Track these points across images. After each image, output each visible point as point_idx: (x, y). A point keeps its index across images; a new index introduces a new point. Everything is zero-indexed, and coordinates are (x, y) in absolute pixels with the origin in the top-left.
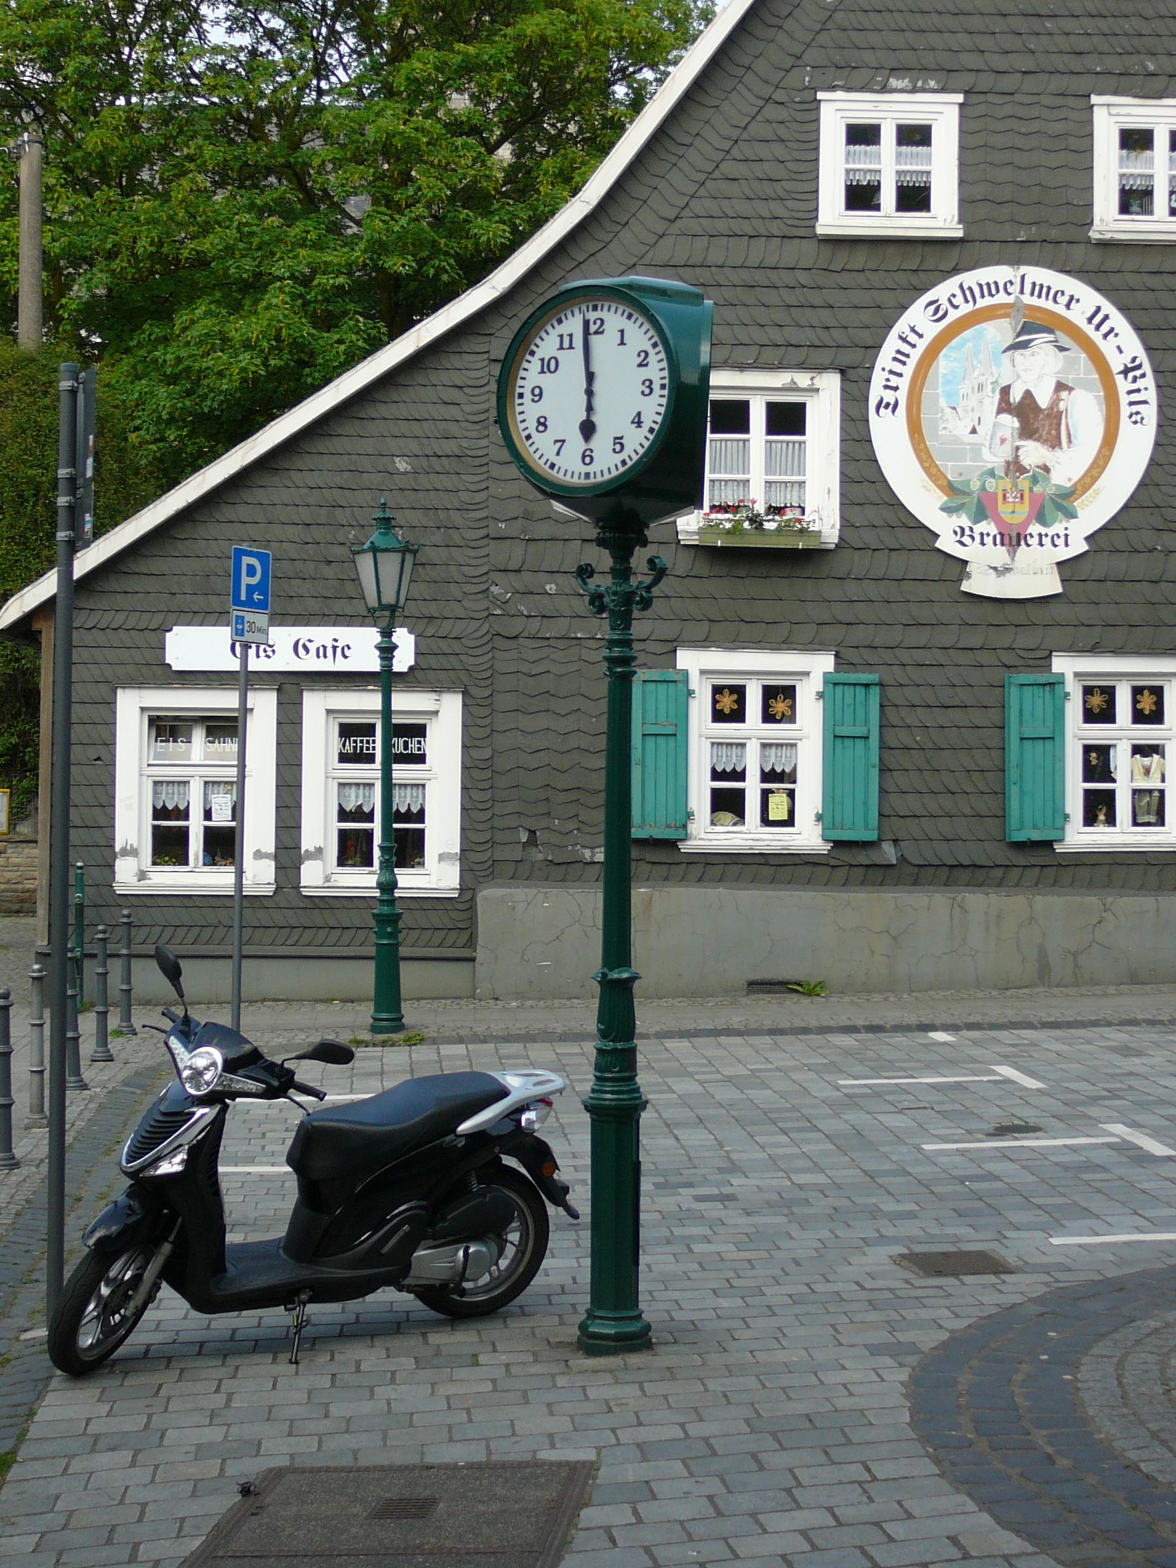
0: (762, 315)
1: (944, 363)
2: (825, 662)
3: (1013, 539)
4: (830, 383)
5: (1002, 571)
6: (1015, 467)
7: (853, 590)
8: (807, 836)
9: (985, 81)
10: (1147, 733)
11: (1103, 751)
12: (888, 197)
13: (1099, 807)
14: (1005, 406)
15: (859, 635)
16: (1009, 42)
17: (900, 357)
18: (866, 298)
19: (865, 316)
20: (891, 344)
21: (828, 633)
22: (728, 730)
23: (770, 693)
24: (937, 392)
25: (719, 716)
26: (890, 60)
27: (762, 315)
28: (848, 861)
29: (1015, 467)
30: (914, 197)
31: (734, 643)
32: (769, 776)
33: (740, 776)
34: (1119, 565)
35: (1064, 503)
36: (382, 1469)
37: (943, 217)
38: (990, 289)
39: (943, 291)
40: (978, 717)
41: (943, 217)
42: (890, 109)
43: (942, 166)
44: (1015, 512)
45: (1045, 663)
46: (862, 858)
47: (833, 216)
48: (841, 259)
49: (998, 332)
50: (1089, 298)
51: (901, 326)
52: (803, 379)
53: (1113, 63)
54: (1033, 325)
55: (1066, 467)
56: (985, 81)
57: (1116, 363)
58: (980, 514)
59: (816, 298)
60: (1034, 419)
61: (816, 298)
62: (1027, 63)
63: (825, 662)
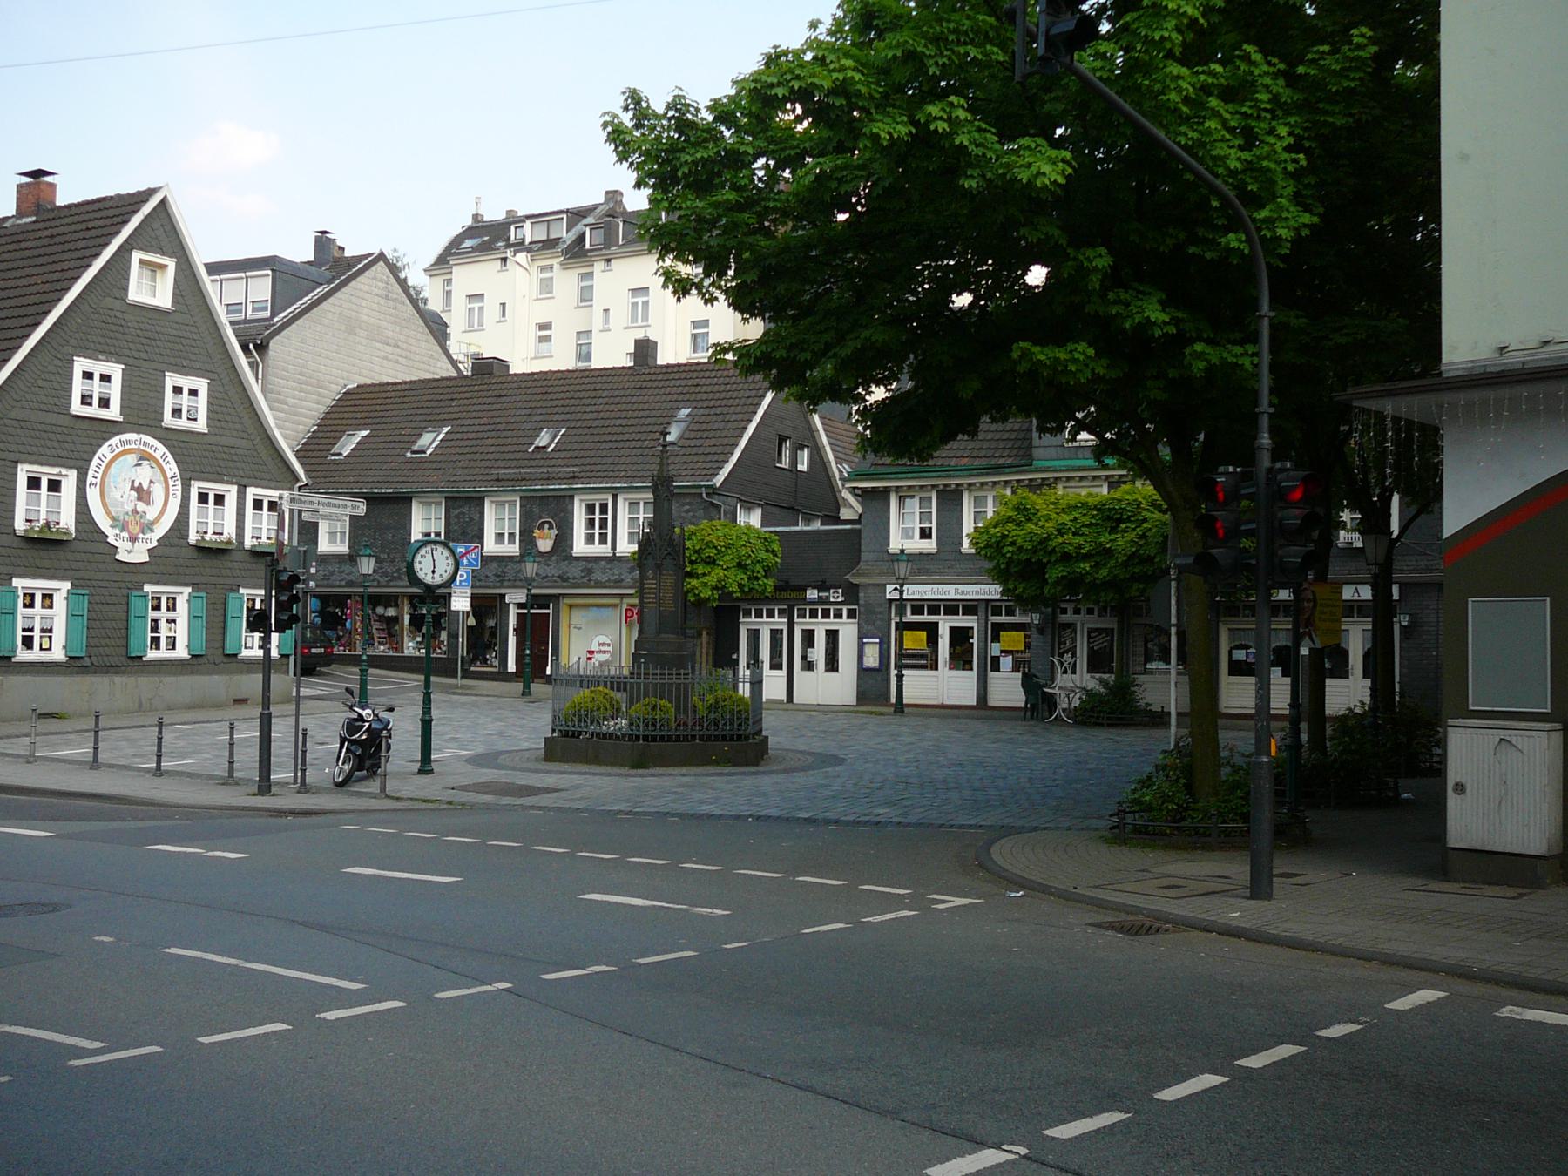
0: (49, 444)
1: (113, 469)
2: (67, 585)
3: (133, 540)
4: (73, 473)
5: (129, 552)
6: (135, 512)
7: (78, 556)
8: (58, 654)
9: (131, 361)
10: (171, 615)
11: (155, 621)
12: (96, 401)
13: (156, 642)
14: (133, 488)
15: (78, 574)
16: (140, 347)
17: (99, 466)
18: (86, 441)
19: (87, 448)
20: (95, 460)
21: (69, 573)
22: (29, 611)
23: (44, 596)
24: (110, 481)
25: (25, 606)
26: (100, 347)
27: (49, 444)
28: (74, 665)
29: (135, 512)
30: (104, 403)
31: (34, 576)
32: (43, 631)
33: (32, 630)
34: (167, 551)
35: (149, 527)
36: (221, 808)
37: (114, 412)
38: (130, 442)
39: (114, 441)
40: (119, 608)
41: (114, 412)
42: (98, 367)
43: (115, 391)
44: (135, 529)
45: (142, 589)
46: (78, 663)
47: (76, 408)
48: (79, 424)
49: (131, 459)
50: (162, 449)
51: (99, 454)
52: (64, 471)
53: (173, 360)
54: (144, 457)
55: (152, 512)
56: (131, 361)
57: (169, 475)
58: (123, 530)
59: (69, 439)
60: (142, 494)
61: (69, 439)
62: (144, 355)
63: (67, 585)
